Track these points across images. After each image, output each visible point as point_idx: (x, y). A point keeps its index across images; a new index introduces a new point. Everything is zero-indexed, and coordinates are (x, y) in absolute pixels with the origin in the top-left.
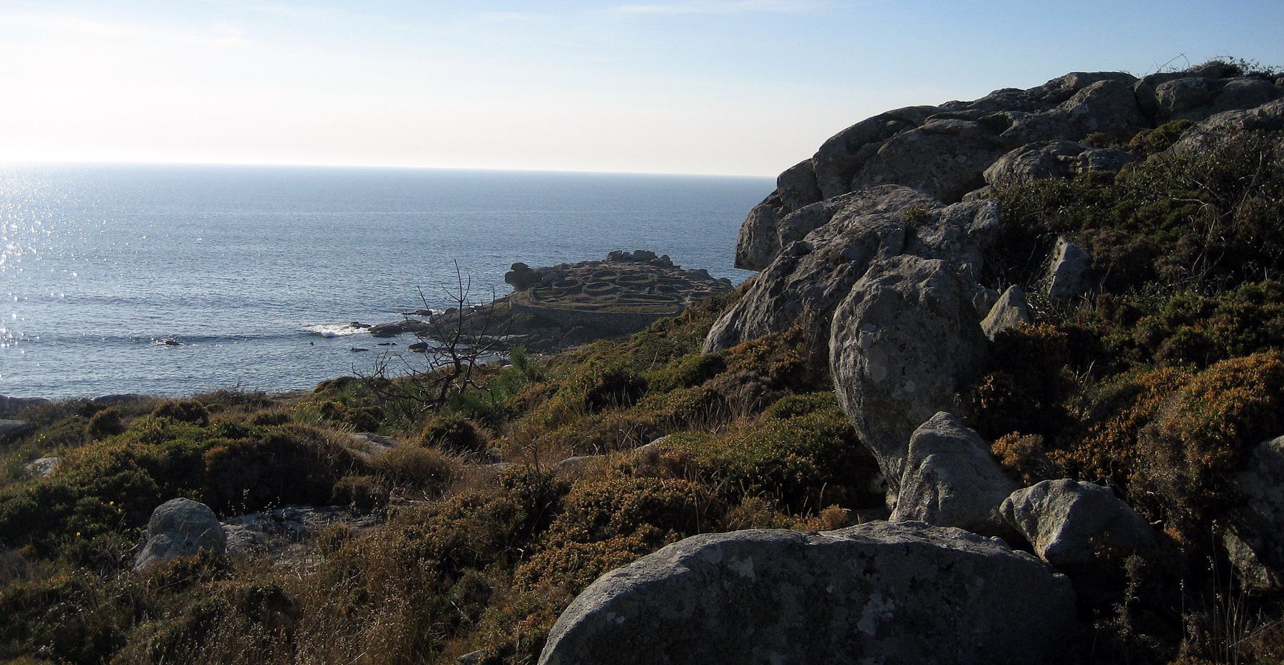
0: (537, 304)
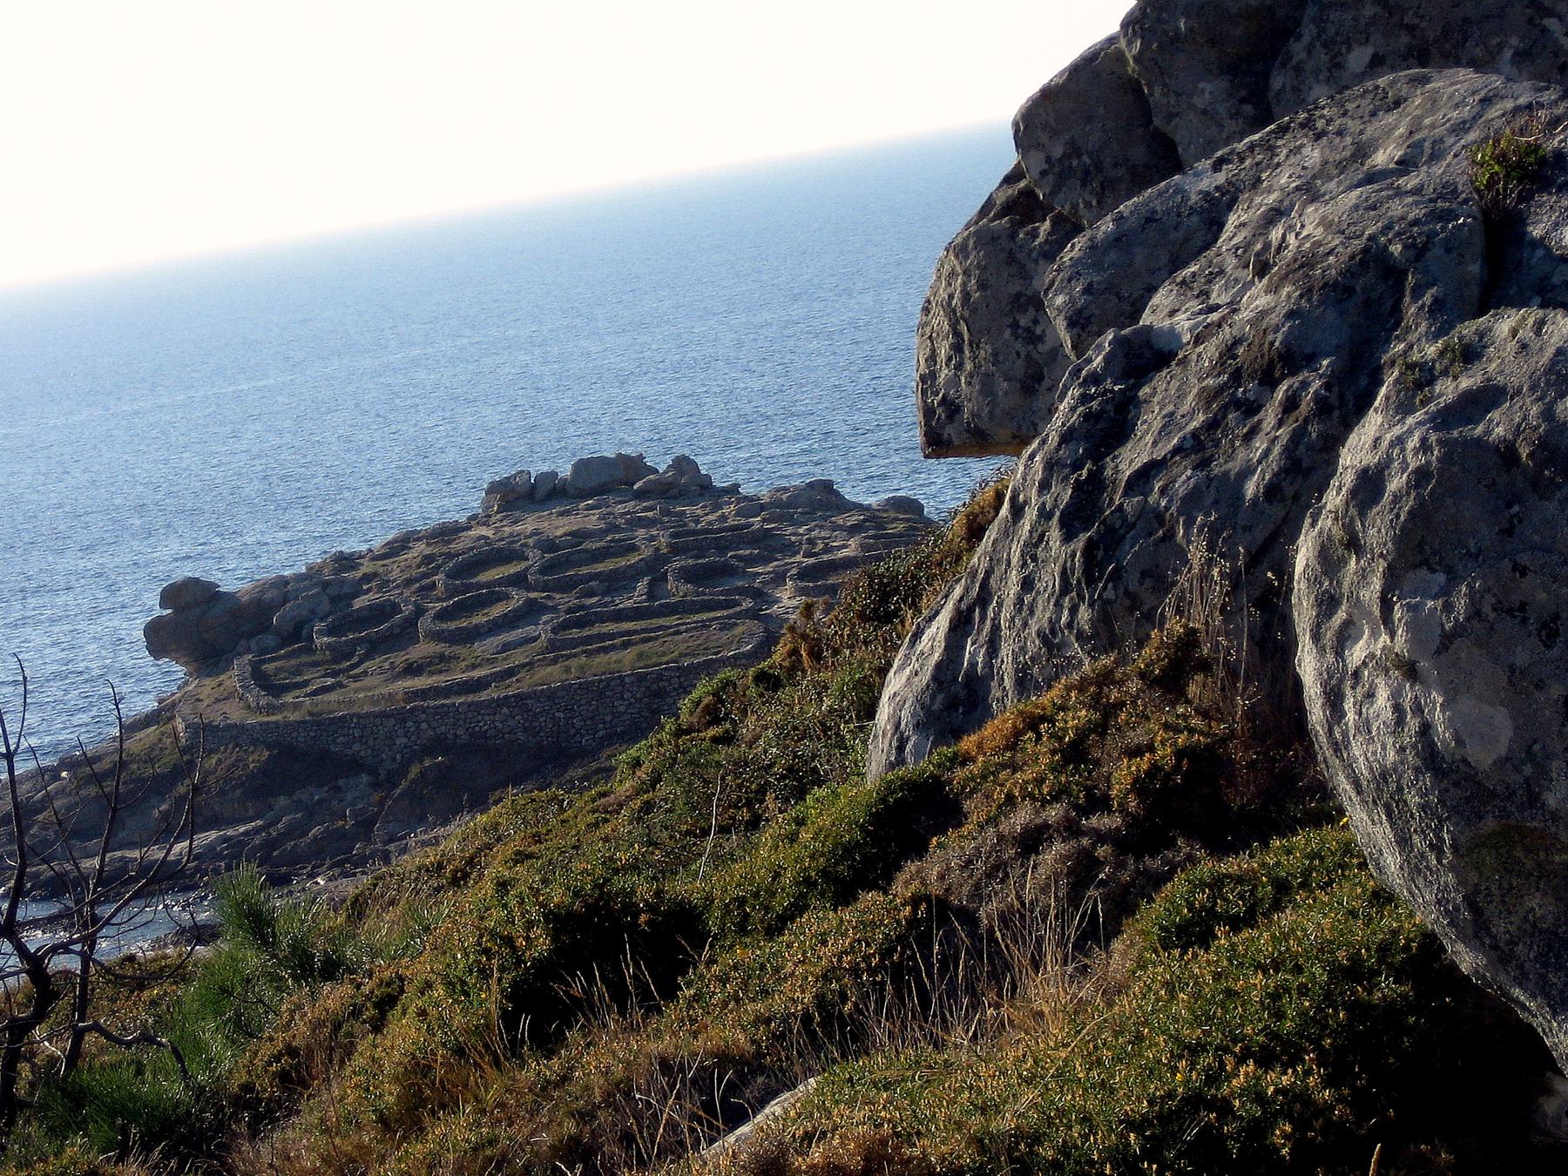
0: (271, 709)
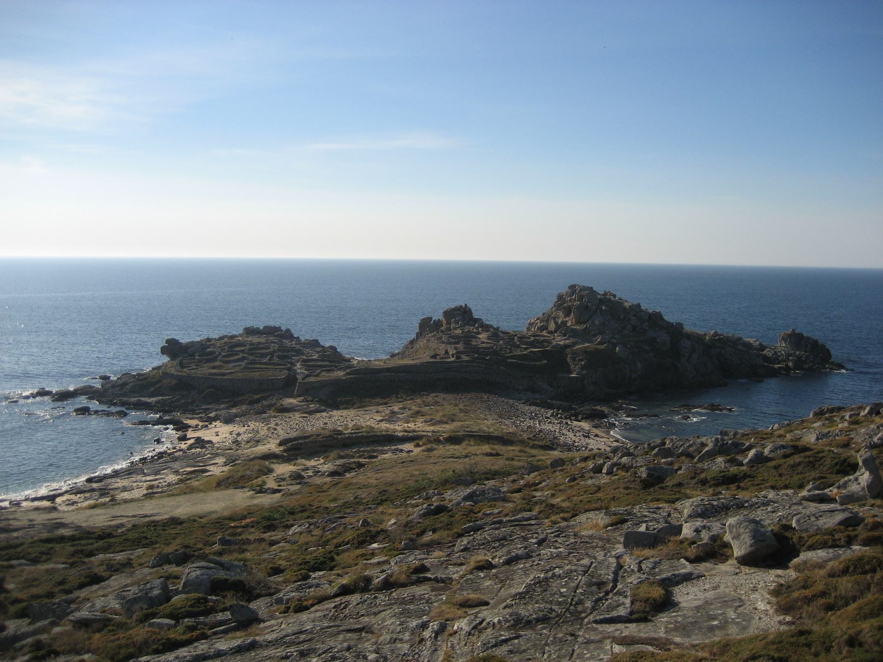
0: (180, 372)
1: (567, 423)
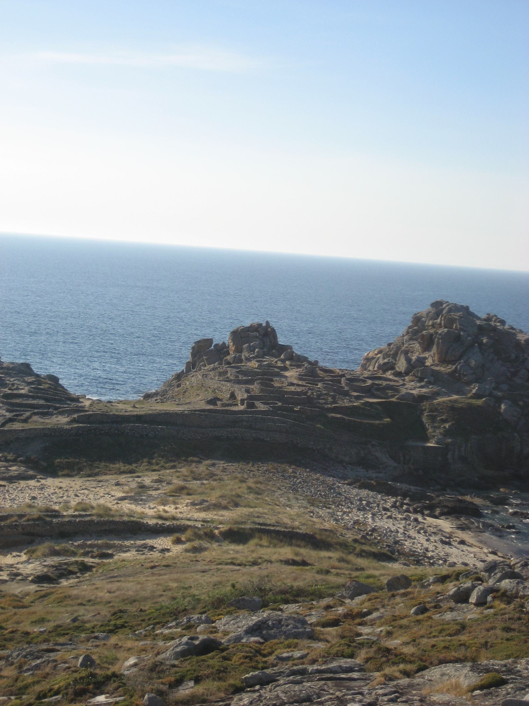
1: (416, 520)
